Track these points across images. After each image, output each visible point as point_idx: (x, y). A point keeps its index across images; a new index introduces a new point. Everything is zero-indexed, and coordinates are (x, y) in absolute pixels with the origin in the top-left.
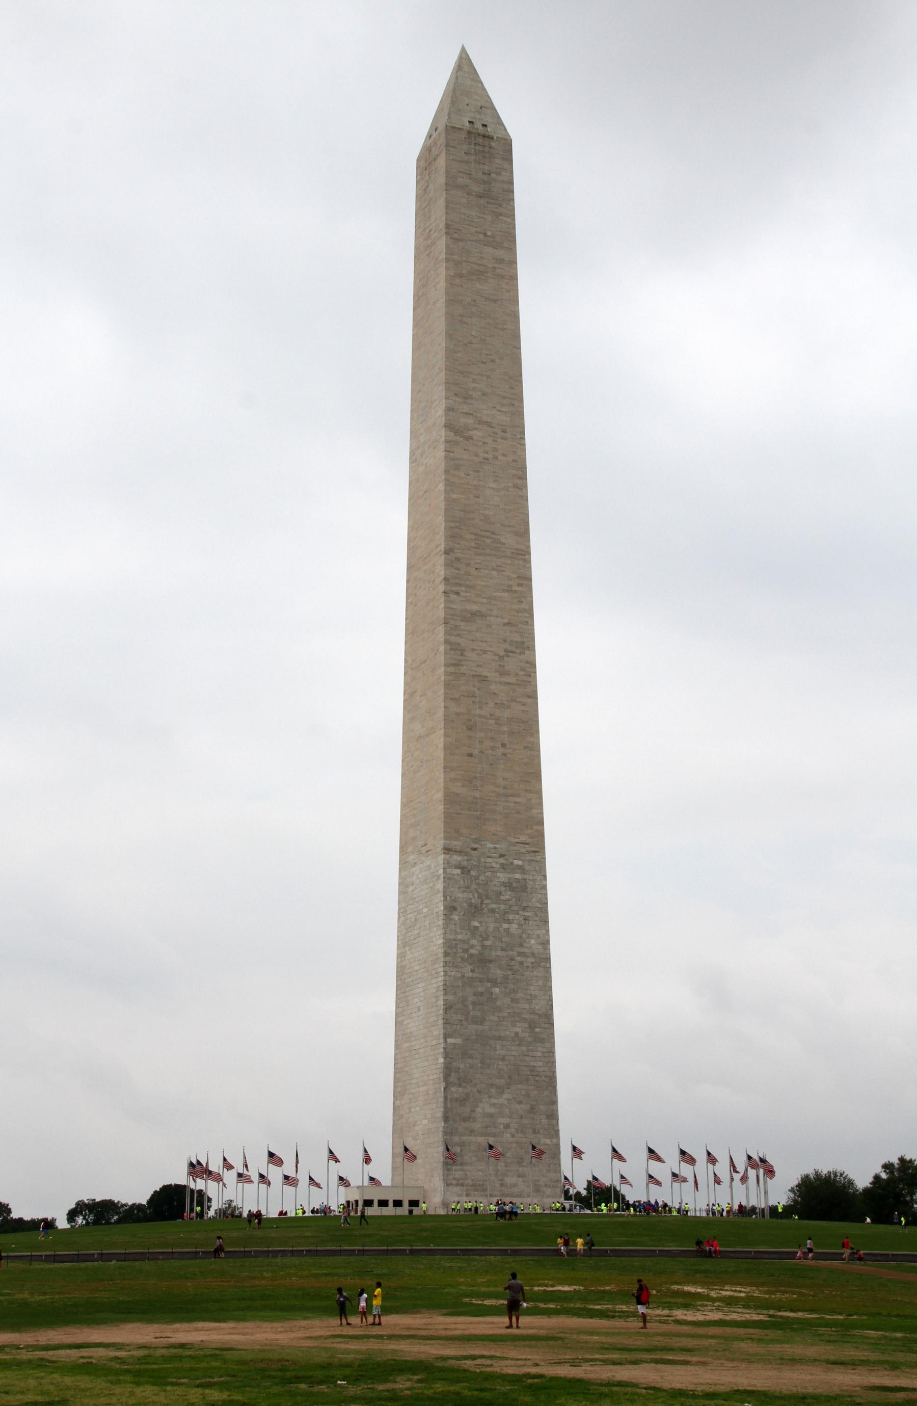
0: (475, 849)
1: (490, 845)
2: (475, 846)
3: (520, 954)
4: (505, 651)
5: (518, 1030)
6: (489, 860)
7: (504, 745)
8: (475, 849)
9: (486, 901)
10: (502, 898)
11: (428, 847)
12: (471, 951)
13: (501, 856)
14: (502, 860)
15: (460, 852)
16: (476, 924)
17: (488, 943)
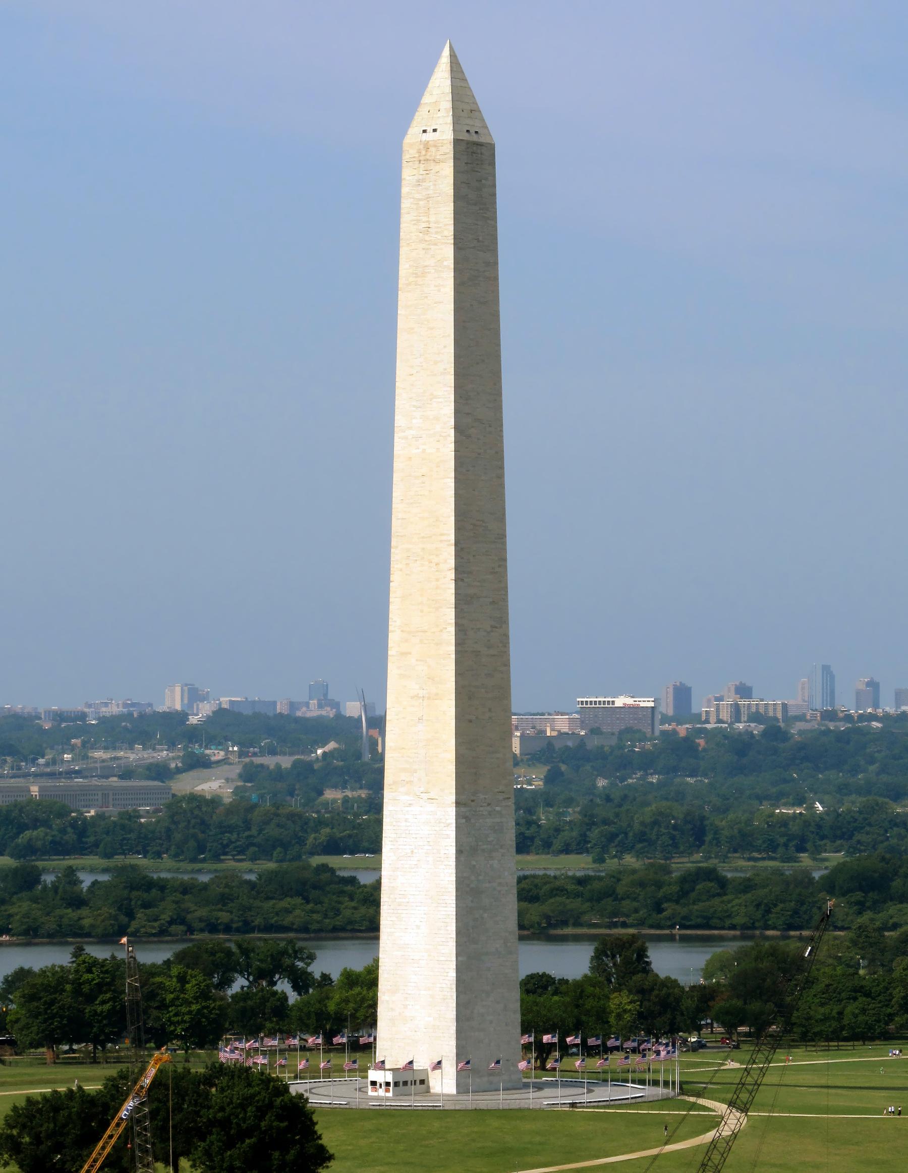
0: (473, 801)
1: (482, 796)
2: (472, 798)
3: (500, 884)
4: (492, 627)
5: (498, 946)
6: (482, 809)
7: (490, 710)
8: (473, 801)
9: (480, 843)
10: (489, 839)
11: (431, 795)
12: (472, 886)
13: (489, 804)
14: (489, 808)
15: (465, 805)
16: (474, 863)
17: (481, 878)
